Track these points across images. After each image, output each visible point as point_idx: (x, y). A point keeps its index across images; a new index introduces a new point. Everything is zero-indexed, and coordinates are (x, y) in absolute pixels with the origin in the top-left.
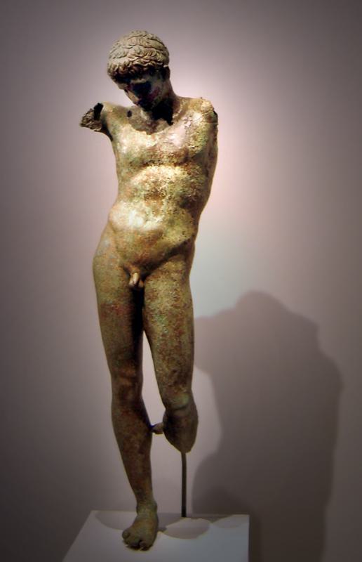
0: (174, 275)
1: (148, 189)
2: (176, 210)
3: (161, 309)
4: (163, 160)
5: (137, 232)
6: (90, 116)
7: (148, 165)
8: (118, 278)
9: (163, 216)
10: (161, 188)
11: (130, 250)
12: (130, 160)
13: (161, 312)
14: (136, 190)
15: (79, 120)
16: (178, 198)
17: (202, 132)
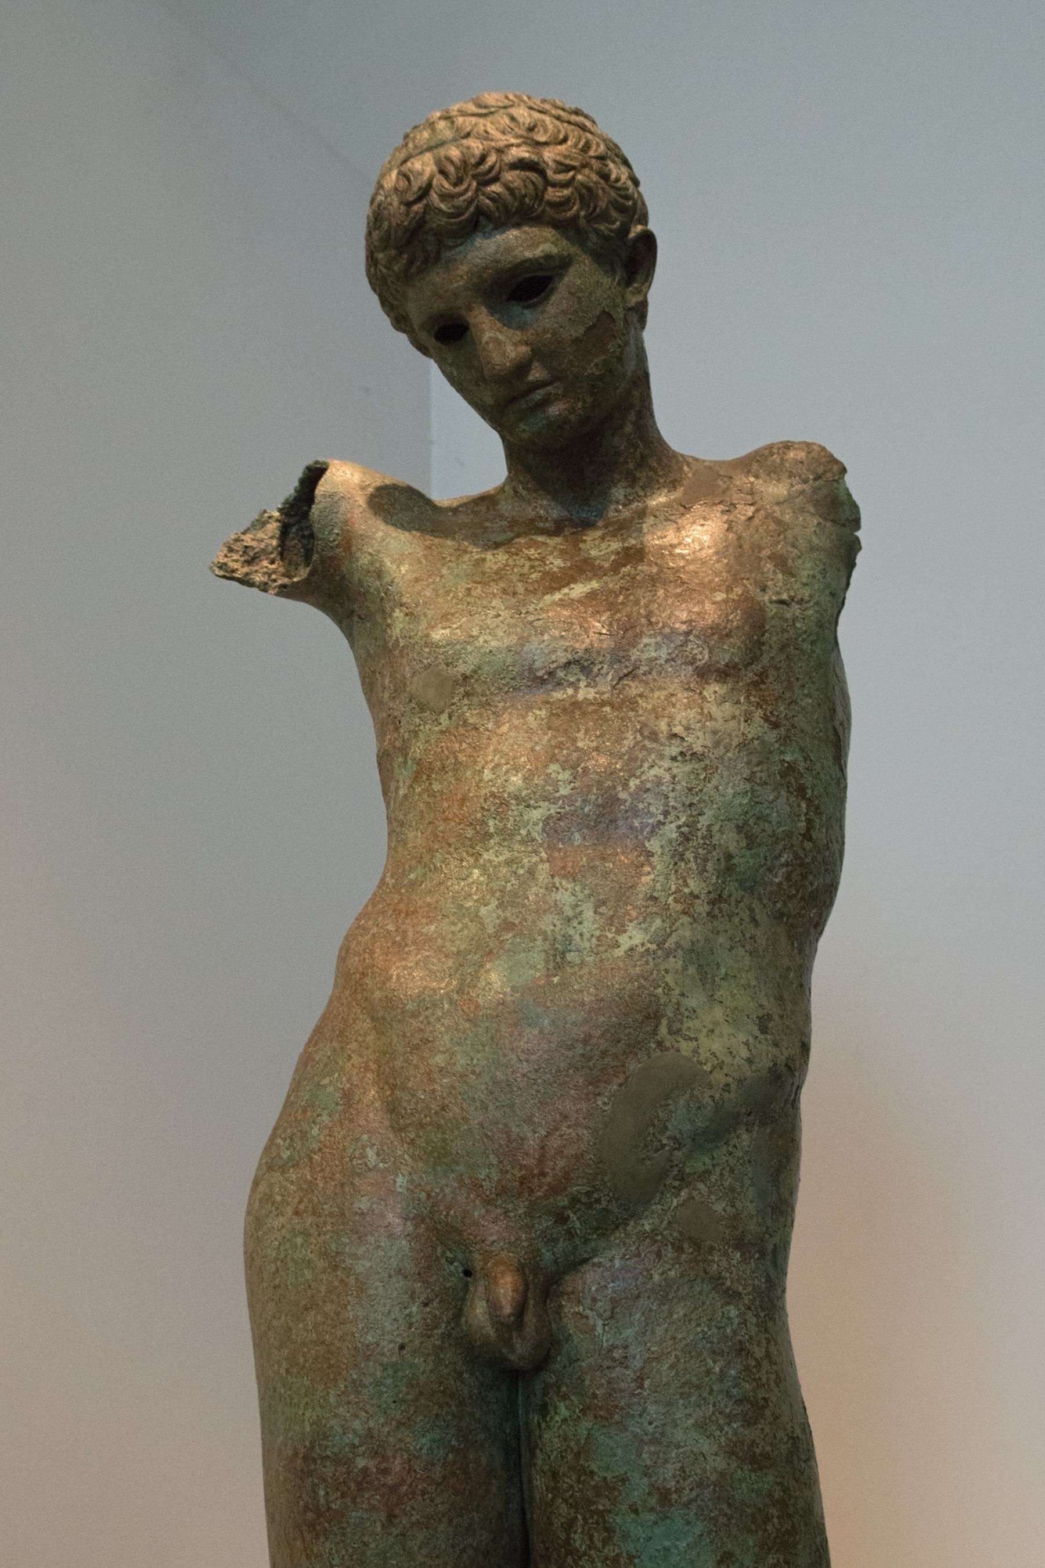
1: (564, 791)
2: (717, 899)
4: (635, 654)
6: (269, 536)
8: (399, 1284)
9: (658, 922)
10: (633, 783)
12: (462, 668)
13: (664, 1497)
16: (730, 840)
17: (812, 549)
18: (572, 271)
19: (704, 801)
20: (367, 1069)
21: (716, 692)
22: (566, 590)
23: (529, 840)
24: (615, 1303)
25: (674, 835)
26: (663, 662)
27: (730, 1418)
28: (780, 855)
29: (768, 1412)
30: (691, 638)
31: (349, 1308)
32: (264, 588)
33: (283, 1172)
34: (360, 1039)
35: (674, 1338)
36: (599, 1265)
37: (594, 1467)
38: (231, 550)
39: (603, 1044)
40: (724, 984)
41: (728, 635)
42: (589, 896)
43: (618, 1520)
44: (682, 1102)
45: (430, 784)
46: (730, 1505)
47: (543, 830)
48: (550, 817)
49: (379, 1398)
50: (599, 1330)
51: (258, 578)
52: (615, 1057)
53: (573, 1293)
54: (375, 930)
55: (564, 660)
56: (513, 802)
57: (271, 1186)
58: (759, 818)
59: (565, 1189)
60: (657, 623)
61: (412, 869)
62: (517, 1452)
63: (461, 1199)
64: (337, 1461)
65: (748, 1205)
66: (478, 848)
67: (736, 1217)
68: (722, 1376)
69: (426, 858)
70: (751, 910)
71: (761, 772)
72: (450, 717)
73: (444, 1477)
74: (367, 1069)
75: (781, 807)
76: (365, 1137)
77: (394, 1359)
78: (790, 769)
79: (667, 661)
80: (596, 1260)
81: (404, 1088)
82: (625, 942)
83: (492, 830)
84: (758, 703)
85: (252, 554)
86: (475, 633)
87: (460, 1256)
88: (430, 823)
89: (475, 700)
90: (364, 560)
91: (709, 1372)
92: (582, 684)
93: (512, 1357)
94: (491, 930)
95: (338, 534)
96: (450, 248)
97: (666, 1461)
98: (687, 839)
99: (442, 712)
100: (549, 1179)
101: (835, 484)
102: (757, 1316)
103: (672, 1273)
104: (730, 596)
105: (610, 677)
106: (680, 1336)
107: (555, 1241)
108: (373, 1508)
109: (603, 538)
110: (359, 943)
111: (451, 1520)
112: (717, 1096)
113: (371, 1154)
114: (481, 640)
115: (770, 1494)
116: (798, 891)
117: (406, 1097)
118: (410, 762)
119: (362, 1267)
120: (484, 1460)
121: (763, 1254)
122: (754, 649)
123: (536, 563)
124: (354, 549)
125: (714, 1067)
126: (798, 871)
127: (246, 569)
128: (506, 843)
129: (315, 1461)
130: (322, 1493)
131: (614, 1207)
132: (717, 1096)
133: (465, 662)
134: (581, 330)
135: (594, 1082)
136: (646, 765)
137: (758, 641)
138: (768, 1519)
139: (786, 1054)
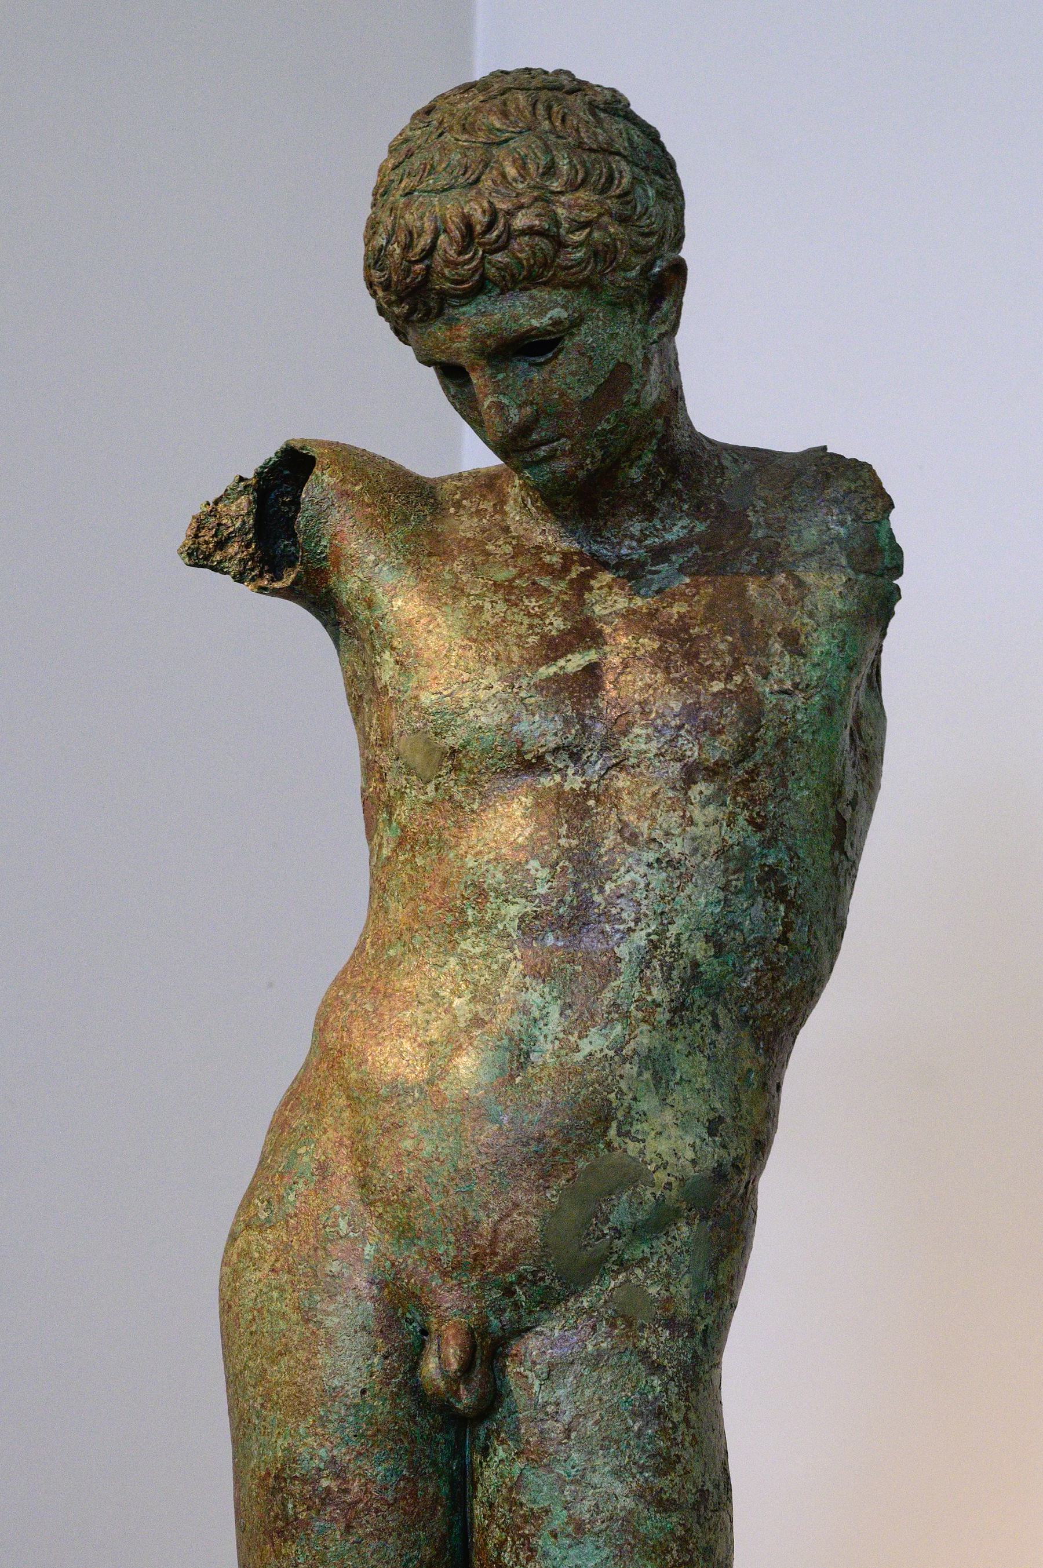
0: (658, 1340)
1: (542, 890)
2: (679, 1008)
3: (583, 1509)
8: (363, 1338)
9: (618, 1028)
12: (450, 741)
13: (580, 1527)
15: (180, 534)
16: (698, 949)
18: (584, 328)
19: (676, 910)
20: (341, 1144)
21: (701, 793)
22: (561, 662)
23: (504, 935)
24: (551, 1367)
25: (643, 943)
26: (651, 755)
27: (642, 1469)
28: (749, 962)
29: (678, 1467)
30: (683, 732)
31: (319, 1356)
33: (261, 1232)
34: (336, 1115)
35: (600, 1400)
36: (541, 1333)
37: (524, 1500)
39: (555, 1143)
40: (678, 1088)
41: (720, 732)
42: (556, 998)
43: (540, 1542)
44: (624, 1197)
45: (414, 856)
46: (634, 1537)
48: (526, 914)
49: (343, 1432)
50: (536, 1388)
52: (566, 1154)
53: (516, 1355)
54: (353, 1007)
55: (552, 745)
56: (492, 894)
57: (249, 1243)
58: (729, 927)
59: (513, 1267)
60: (651, 712)
61: (392, 945)
62: (461, 1486)
63: (421, 1269)
64: (304, 1481)
65: (683, 1289)
66: (456, 935)
67: (670, 1299)
68: (639, 1435)
69: (406, 937)
70: (714, 1014)
71: (737, 880)
72: (437, 789)
73: (395, 1499)
74: (341, 1144)
75: (756, 915)
76: (338, 1208)
77: (357, 1401)
78: (772, 872)
79: (656, 755)
80: (538, 1329)
82: (586, 1047)
83: (470, 919)
84: (745, 804)
86: (465, 705)
87: (419, 1318)
88: (411, 899)
90: (352, 584)
91: (628, 1429)
92: (570, 772)
93: (459, 1406)
94: (462, 1025)
95: (325, 547)
96: (454, 307)
97: (583, 1499)
98: (656, 948)
99: (429, 782)
100: (499, 1258)
101: (877, 527)
102: (680, 1386)
103: (604, 1345)
104: (730, 686)
105: (598, 767)
106: (605, 1398)
107: (504, 1310)
108: (333, 1520)
109: (610, 587)
110: (337, 1018)
111: (400, 1535)
112: (658, 1194)
113: (343, 1224)
114: (471, 713)
115: (672, 1532)
116: (767, 994)
117: (376, 1175)
118: (394, 824)
119: (331, 1322)
120: (431, 1490)
121: (692, 1333)
122: (746, 749)
123: (537, 621)
124: (343, 569)
125: (658, 1168)
126: (770, 975)
128: (482, 936)
129: (285, 1480)
130: (290, 1506)
131: (556, 1285)
132: (658, 1194)
133: (453, 735)
134: (592, 389)
135: (545, 1175)
136: (623, 869)
137: (752, 737)
138: (668, 1551)
139: (733, 1154)
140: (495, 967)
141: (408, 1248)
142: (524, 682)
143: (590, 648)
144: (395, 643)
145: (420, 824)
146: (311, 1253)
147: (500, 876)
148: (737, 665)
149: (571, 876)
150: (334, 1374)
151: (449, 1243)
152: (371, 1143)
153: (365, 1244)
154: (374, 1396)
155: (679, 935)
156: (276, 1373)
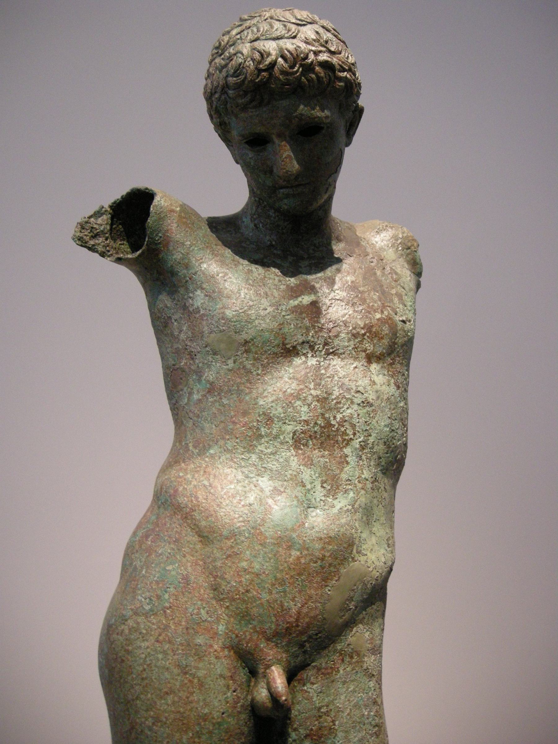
4: (336, 342)
5: (285, 541)
7: (297, 354)
8: (222, 682)
9: (351, 494)
10: (339, 416)
11: (265, 596)
12: (244, 336)
14: (269, 420)
15: (71, 229)
22: (300, 299)
30: (366, 337)
31: (194, 695)
32: (103, 255)
33: (147, 617)
35: (349, 700)
38: (83, 228)
40: (375, 524)
41: (382, 338)
47: (293, 438)
51: (100, 249)
53: (301, 680)
55: (301, 341)
56: (276, 419)
59: (306, 632)
61: (210, 447)
63: (255, 638)
66: (255, 442)
67: (372, 639)
72: (234, 362)
77: (219, 720)
80: (313, 664)
81: (223, 578)
83: (263, 433)
85: (95, 232)
86: (253, 318)
89: (251, 356)
90: (177, 256)
92: (309, 355)
95: (161, 237)
98: (364, 449)
99: (229, 358)
100: (300, 628)
103: (348, 669)
106: (351, 699)
114: (257, 322)
118: (204, 382)
119: (201, 673)
127: (92, 242)
128: (271, 442)
133: (246, 333)
136: (346, 407)
140: (281, 460)
141: (246, 625)
142: (284, 307)
143: (311, 294)
144: (204, 286)
145: (224, 381)
146: (185, 631)
147: (280, 410)
148: (384, 306)
149: (319, 410)
150: (206, 705)
151: (272, 622)
152: (219, 564)
153: (219, 625)
154: (229, 716)
155: (374, 442)
156: (161, 705)
